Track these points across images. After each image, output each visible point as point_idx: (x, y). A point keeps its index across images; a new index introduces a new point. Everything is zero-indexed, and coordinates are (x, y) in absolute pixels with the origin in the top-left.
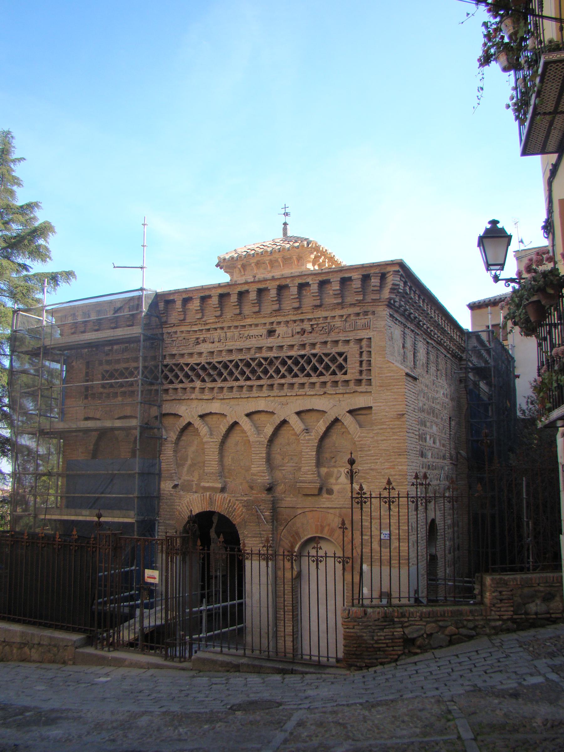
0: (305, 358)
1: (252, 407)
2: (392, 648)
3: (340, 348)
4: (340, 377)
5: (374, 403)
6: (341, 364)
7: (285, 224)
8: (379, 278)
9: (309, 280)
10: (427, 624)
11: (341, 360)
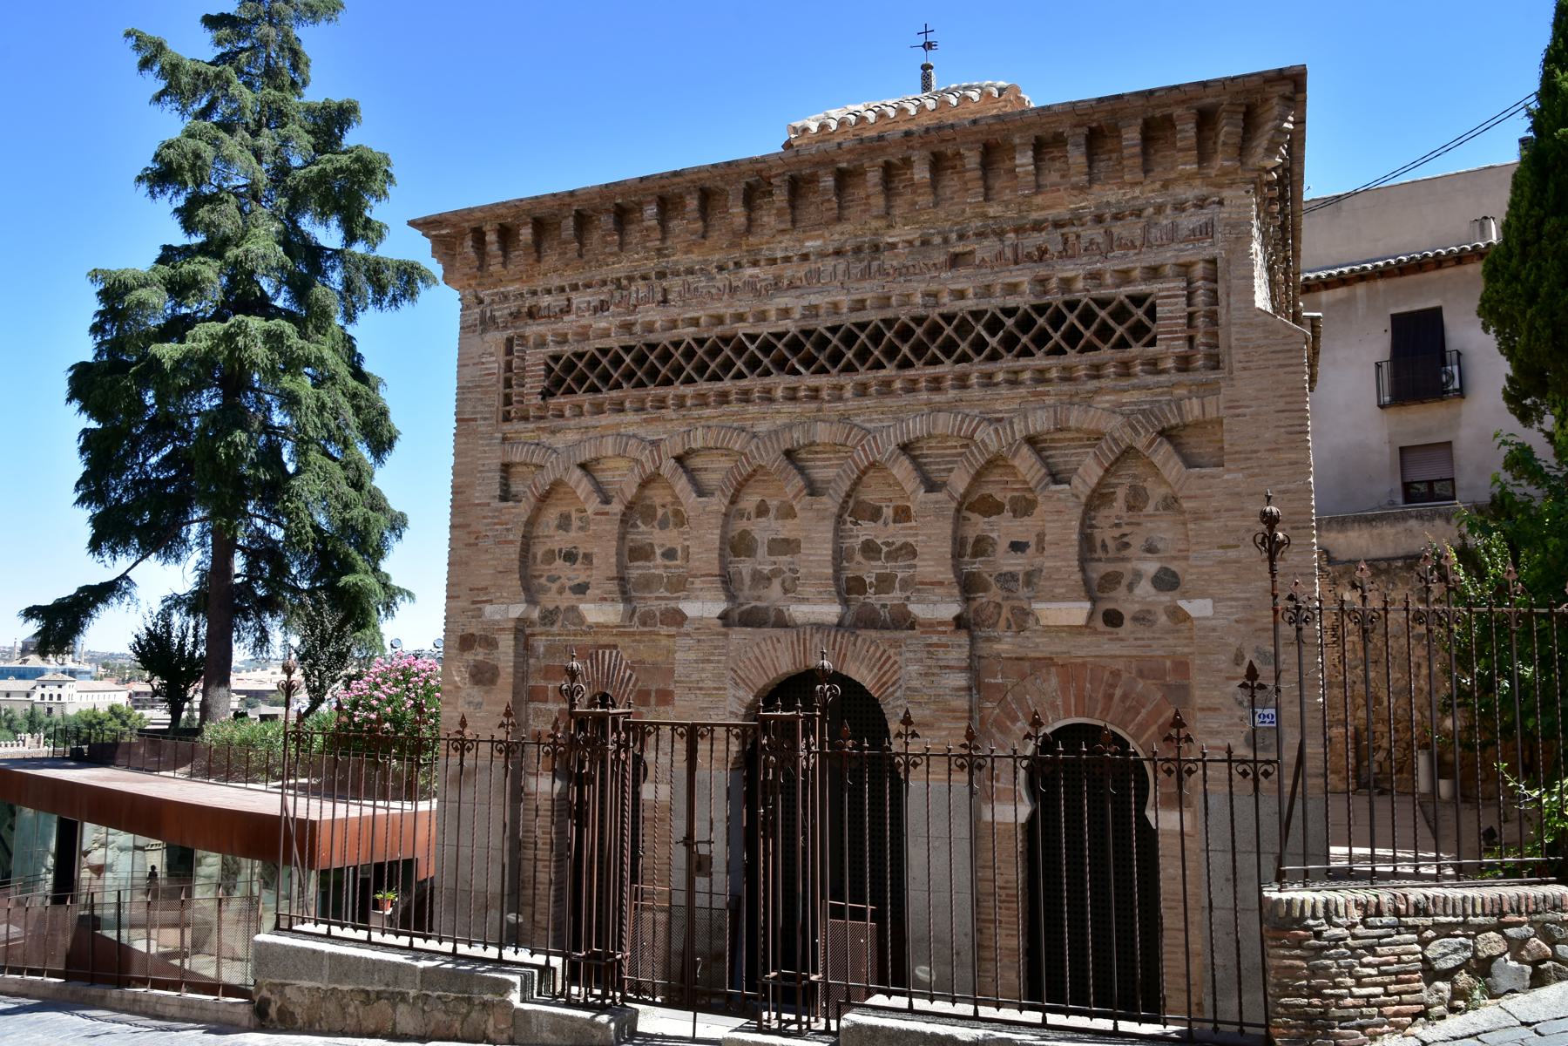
1: (916, 427)
2: (1396, 998)
3: (1142, 288)
4: (1136, 350)
6: (1139, 321)
7: (926, 68)
8: (1241, 116)
9: (1065, 129)
10: (1478, 933)
11: (1139, 313)
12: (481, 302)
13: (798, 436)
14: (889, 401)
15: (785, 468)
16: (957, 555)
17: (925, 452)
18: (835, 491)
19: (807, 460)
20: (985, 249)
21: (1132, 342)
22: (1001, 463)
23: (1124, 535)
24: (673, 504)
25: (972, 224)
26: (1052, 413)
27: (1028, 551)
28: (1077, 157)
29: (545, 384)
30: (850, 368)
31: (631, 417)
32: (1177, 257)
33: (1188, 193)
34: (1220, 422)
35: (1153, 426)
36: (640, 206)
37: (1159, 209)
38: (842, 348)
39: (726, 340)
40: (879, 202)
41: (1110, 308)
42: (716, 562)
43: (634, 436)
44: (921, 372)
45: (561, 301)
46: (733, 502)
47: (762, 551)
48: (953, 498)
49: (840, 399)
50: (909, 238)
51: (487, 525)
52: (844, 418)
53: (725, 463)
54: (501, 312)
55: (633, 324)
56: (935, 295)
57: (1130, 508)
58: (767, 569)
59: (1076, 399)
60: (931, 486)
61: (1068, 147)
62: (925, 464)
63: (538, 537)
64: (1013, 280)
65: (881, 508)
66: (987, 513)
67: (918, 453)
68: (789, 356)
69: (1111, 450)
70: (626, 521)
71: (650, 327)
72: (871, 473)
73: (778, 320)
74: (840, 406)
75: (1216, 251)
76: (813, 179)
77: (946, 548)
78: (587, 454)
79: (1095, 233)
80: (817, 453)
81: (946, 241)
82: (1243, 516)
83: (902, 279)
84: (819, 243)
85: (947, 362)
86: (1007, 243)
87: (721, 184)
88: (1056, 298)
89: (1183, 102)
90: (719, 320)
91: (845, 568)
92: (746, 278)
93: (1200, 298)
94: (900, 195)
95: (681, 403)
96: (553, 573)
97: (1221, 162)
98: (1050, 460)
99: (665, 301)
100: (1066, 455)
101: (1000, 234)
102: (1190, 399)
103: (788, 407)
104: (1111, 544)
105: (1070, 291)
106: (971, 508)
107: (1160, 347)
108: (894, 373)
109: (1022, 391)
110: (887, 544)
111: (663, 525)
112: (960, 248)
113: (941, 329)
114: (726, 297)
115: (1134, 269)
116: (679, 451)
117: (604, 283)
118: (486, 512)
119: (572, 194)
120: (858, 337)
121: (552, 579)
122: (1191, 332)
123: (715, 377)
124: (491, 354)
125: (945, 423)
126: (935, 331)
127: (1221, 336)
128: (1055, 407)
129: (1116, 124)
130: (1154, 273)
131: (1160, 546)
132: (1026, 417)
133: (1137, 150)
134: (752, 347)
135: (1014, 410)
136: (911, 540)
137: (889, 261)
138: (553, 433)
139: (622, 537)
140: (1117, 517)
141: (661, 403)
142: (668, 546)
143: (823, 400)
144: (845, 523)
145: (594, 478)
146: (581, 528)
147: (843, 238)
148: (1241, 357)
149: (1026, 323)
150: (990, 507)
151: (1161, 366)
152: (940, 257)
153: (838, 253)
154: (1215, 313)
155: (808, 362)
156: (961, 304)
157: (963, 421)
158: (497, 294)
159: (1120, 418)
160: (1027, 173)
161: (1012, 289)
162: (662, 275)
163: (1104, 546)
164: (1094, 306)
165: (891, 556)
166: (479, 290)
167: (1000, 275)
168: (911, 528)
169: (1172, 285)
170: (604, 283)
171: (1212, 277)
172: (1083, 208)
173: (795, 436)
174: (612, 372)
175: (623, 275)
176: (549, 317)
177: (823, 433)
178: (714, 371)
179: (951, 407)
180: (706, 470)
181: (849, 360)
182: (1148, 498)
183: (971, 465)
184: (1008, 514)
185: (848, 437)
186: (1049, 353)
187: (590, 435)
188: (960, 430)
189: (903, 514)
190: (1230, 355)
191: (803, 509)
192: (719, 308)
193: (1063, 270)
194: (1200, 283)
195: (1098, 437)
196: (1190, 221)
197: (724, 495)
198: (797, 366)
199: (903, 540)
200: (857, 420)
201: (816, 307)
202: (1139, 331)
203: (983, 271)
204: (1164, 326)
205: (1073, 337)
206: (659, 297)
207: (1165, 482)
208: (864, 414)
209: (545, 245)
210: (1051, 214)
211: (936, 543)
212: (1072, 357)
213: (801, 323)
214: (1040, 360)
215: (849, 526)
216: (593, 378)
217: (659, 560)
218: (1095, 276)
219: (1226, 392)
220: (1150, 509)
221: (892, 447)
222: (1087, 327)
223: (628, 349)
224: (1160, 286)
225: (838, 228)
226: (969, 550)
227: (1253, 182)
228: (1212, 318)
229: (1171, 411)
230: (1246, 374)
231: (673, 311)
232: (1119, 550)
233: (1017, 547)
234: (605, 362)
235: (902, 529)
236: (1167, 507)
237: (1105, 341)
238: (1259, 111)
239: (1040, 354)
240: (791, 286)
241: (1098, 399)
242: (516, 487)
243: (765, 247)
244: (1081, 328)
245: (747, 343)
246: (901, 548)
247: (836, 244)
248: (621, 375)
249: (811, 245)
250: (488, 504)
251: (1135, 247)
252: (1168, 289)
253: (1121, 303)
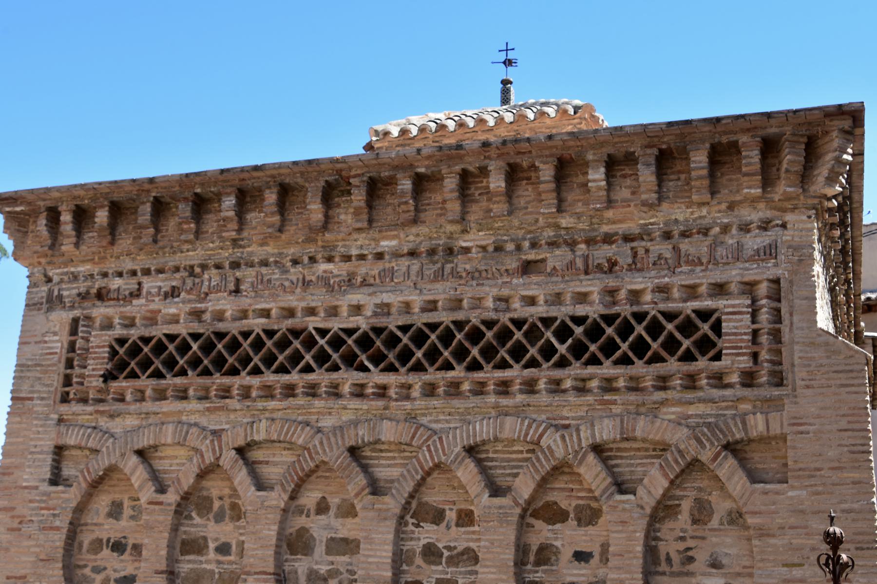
0: (618, 321)
1: (482, 430)
3: (707, 304)
4: (702, 363)
5: (790, 425)
6: (705, 336)
7: (506, 82)
8: (803, 146)
11: (705, 328)
12: (49, 280)
13: (363, 434)
14: (456, 403)
15: (349, 465)
16: (520, 563)
17: (491, 455)
18: (398, 490)
19: (371, 458)
20: (556, 258)
21: (697, 354)
22: (566, 470)
23: (689, 549)
24: (230, 496)
25: (545, 234)
26: (618, 420)
27: (592, 561)
28: (647, 175)
29: (109, 367)
30: (418, 368)
31: (193, 405)
32: (742, 276)
33: (754, 216)
34: (783, 438)
35: (718, 440)
36: (218, 197)
37: (725, 229)
38: (412, 347)
39: (296, 333)
40: (454, 207)
41: (677, 321)
42: (272, 559)
43: (196, 425)
44: (490, 375)
45: (130, 284)
46: (293, 498)
47: (320, 550)
48: (517, 504)
49: (408, 398)
50: (484, 243)
51: (33, 509)
52: (411, 418)
53: (288, 457)
54: (69, 292)
55: (203, 312)
56: (506, 300)
57: (695, 522)
58: (323, 569)
59: (643, 410)
60: (496, 491)
61: (639, 166)
62: (490, 468)
63: (86, 524)
64: (583, 290)
65: (444, 510)
66: (551, 521)
67: (483, 456)
68: (359, 353)
69: (676, 462)
70: (180, 512)
71: (219, 316)
72: (435, 475)
73: (349, 316)
74: (408, 405)
75: (779, 272)
76: (391, 182)
77: (509, 555)
78: (144, 441)
79: (664, 249)
80: (381, 451)
81: (519, 248)
82: (807, 534)
83: (474, 283)
84: (394, 243)
85: (517, 367)
86: (579, 253)
87: (300, 180)
88: (625, 310)
89: (748, 130)
90: (290, 313)
91: (404, 572)
92: (320, 273)
93: (764, 316)
94: (477, 201)
95: (246, 393)
96: (98, 563)
97: (784, 188)
98: (616, 470)
99: (237, 291)
100: (632, 465)
101: (572, 245)
102: (754, 414)
103: (355, 404)
104: (676, 558)
105: (638, 303)
106: (535, 515)
107: (725, 362)
108: (462, 374)
109: (590, 398)
110: (449, 548)
111: (219, 518)
112: (532, 256)
113: (511, 334)
114: (298, 290)
115: (701, 285)
116: (241, 442)
117: (177, 269)
118: (34, 495)
119: (151, 180)
120: (429, 337)
121: (97, 570)
122: (756, 349)
123: (283, 370)
124: (55, 334)
125: (511, 427)
126: (504, 335)
127: (784, 354)
128: (621, 416)
129: (685, 147)
130: (720, 289)
131: (725, 561)
132: (593, 425)
133: (705, 172)
134: (322, 342)
135: (582, 418)
136: (473, 545)
137: (463, 264)
138: (112, 416)
139: (175, 529)
140: (683, 530)
141: (225, 393)
142: (223, 540)
143: (390, 398)
144: (406, 524)
145: (150, 466)
146: (132, 517)
147: (418, 240)
148: (804, 375)
149: (595, 332)
150: (555, 515)
151: (727, 380)
152: (512, 264)
153: (412, 254)
154: (779, 331)
155: (378, 359)
156: (532, 310)
157: (530, 426)
158: (66, 273)
159: (686, 430)
160: (599, 188)
161: (582, 298)
162: (235, 265)
163: (669, 560)
164: (661, 318)
165: (453, 561)
166: (48, 268)
167: (572, 284)
168: (474, 532)
169: (737, 302)
170: (177, 269)
171: (776, 296)
172: (652, 224)
173: (360, 433)
174: (178, 358)
175: (196, 262)
176: (118, 299)
177: (388, 432)
178: (282, 363)
179: (518, 412)
180: (267, 463)
181: (419, 360)
182: (713, 513)
183: (537, 471)
184: (572, 522)
185: (413, 437)
186: (616, 363)
187: (150, 421)
188: (527, 435)
189: (466, 518)
190: (793, 372)
191: (364, 508)
192: (292, 301)
193: (631, 283)
194: (764, 302)
195: (665, 448)
196: (754, 241)
197: (284, 490)
198: (367, 363)
199: (465, 545)
200: (424, 420)
201: (388, 305)
202: (705, 345)
203: (554, 279)
204: (730, 341)
205: (640, 348)
206: (232, 286)
207: (730, 496)
208: (431, 414)
209: (121, 229)
210: (622, 228)
211: (499, 550)
212: (639, 368)
213: (372, 321)
214: (608, 369)
215: (411, 527)
216: (158, 364)
217: (212, 555)
218: (663, 290)
219: (789, 409)
220: (715, 523)
221: (458, 449)
222: (655, 339)
223: (196, 336)
224: (725, 302)
225: (414, 230)
226: (532, 558)
227: (814, 208)
228: (776, 335)
229: (736, 424)
230: (809, 392)
231: (244, 302)
232: (683, 564)
233: (581, 557)
234: (171, 347)
235: (465, 533)
236: (731, 522)
237: (672, 353)
238: (820, 142)
239: (607, 363)
240: (364, 283)
241: (665, 410)
242: (67, 471)
243: (340, 244)
244: (648, 339)
245: (317, 338)
246: (462, 553)
247: (411, 246)
248: (187, 362)
249: (386, 244)
250: (36, 488)
251: (702, 264)
252: (733, 306)
253: (688, 317)
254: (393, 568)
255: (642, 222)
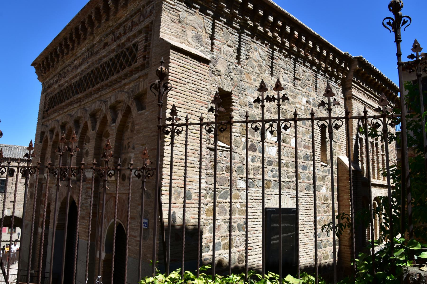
215: (85, 145)
224: (140, 38)
254: (77, 159)
255: (126, 15)
